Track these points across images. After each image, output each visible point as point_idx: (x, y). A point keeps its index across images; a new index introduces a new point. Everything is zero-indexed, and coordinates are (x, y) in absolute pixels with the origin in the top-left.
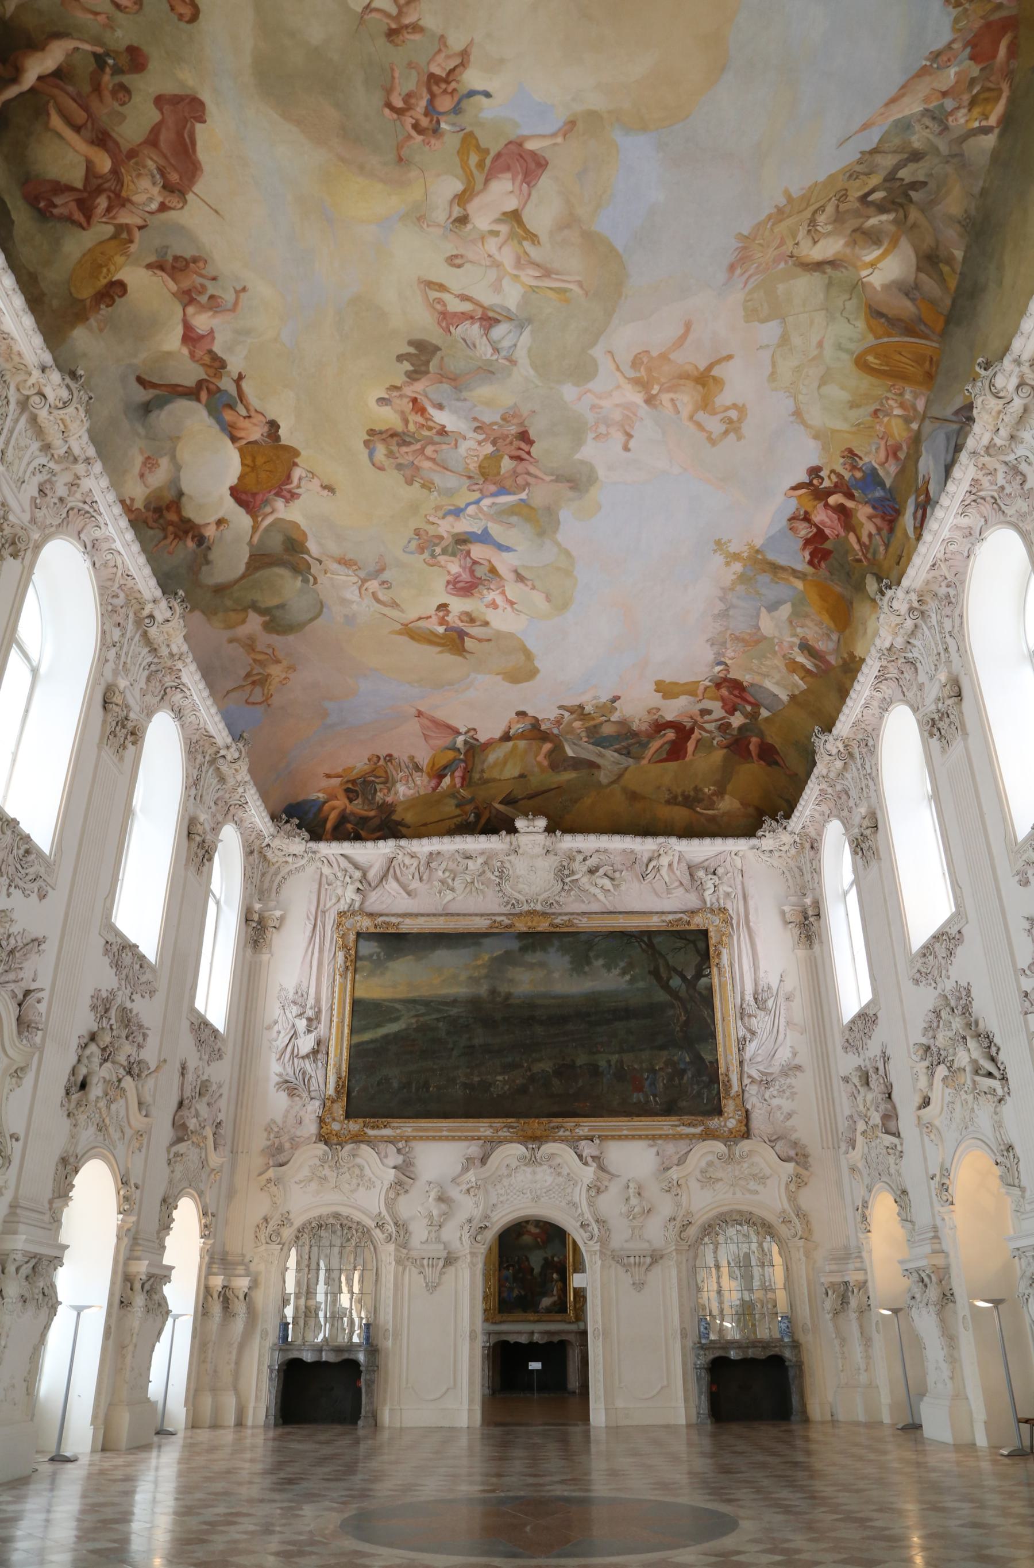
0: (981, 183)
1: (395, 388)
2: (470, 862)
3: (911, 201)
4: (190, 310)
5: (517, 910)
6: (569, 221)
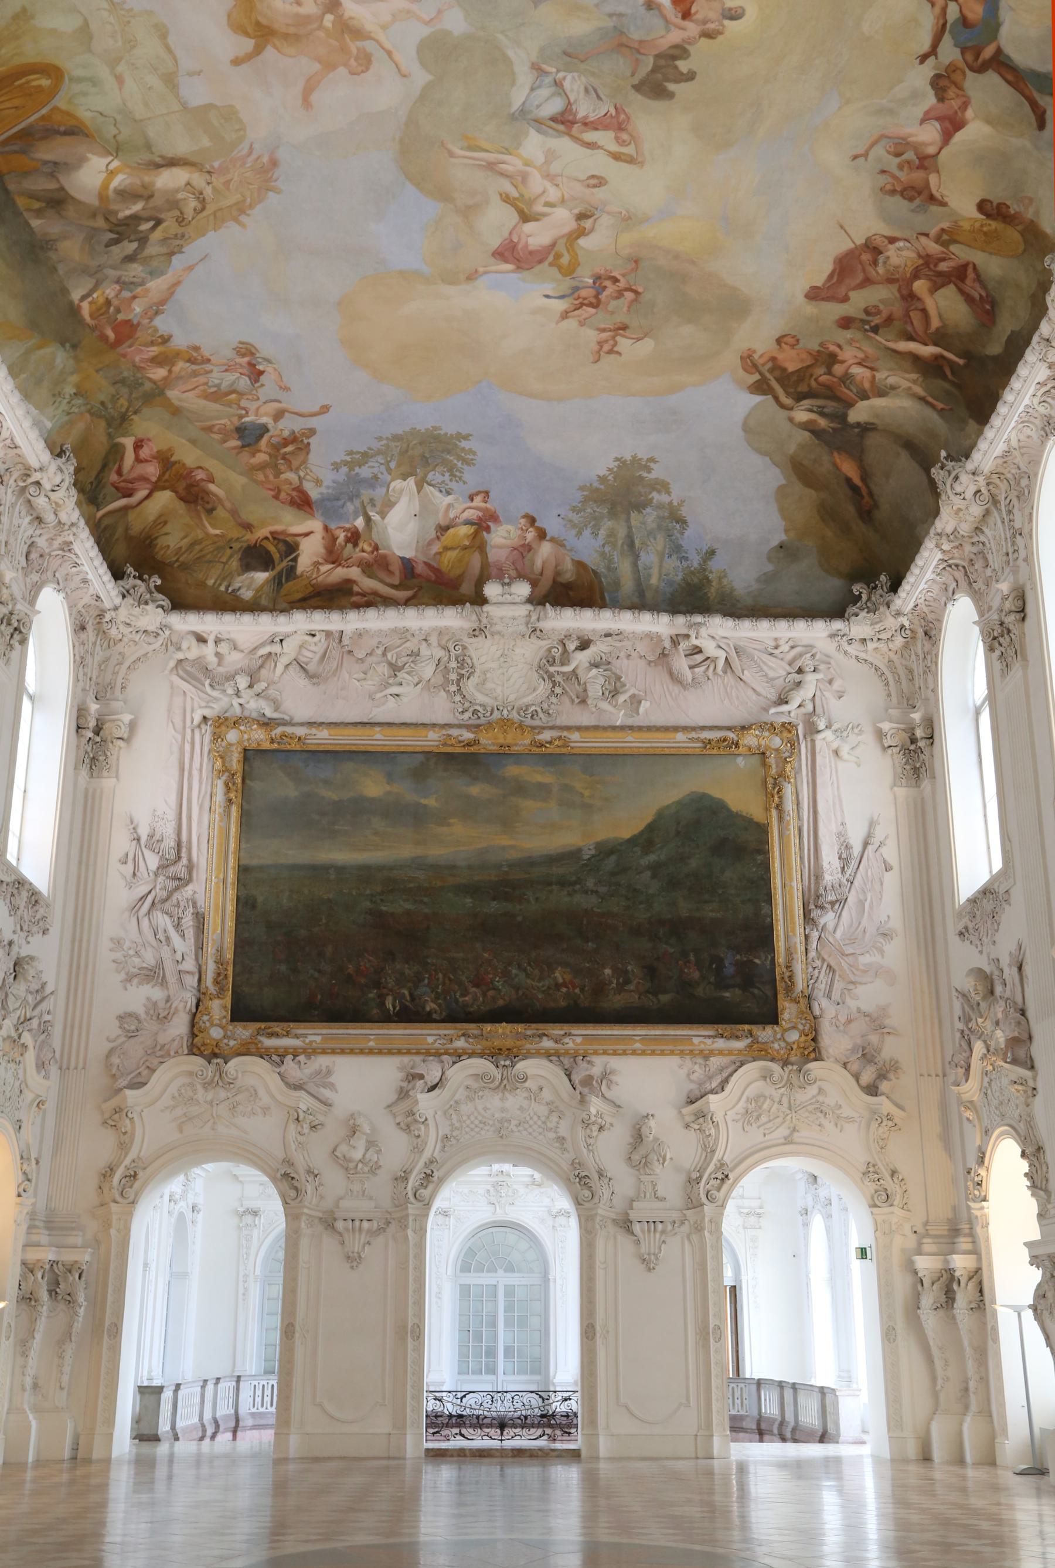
0: (61, 272)
1: (709, 35)
3: (111, 231)
4: (931, 150)
6: (469, 211)
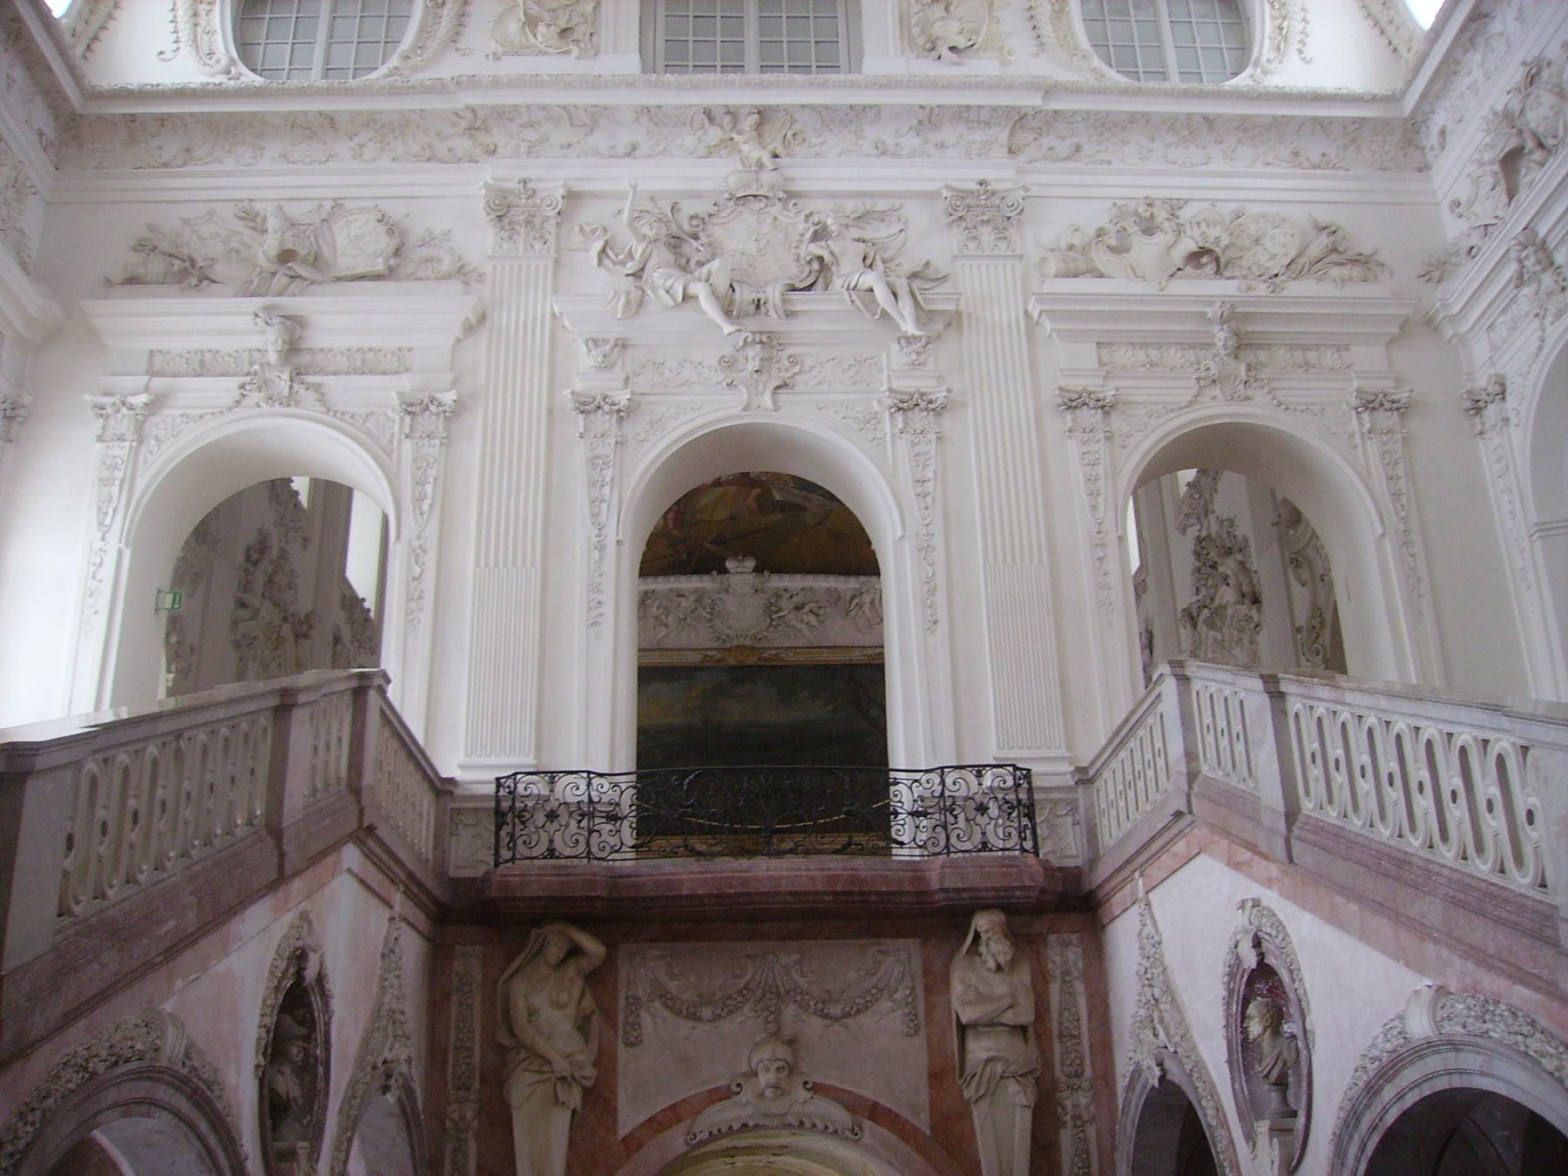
2: (683, 602)
5: (728, 645)
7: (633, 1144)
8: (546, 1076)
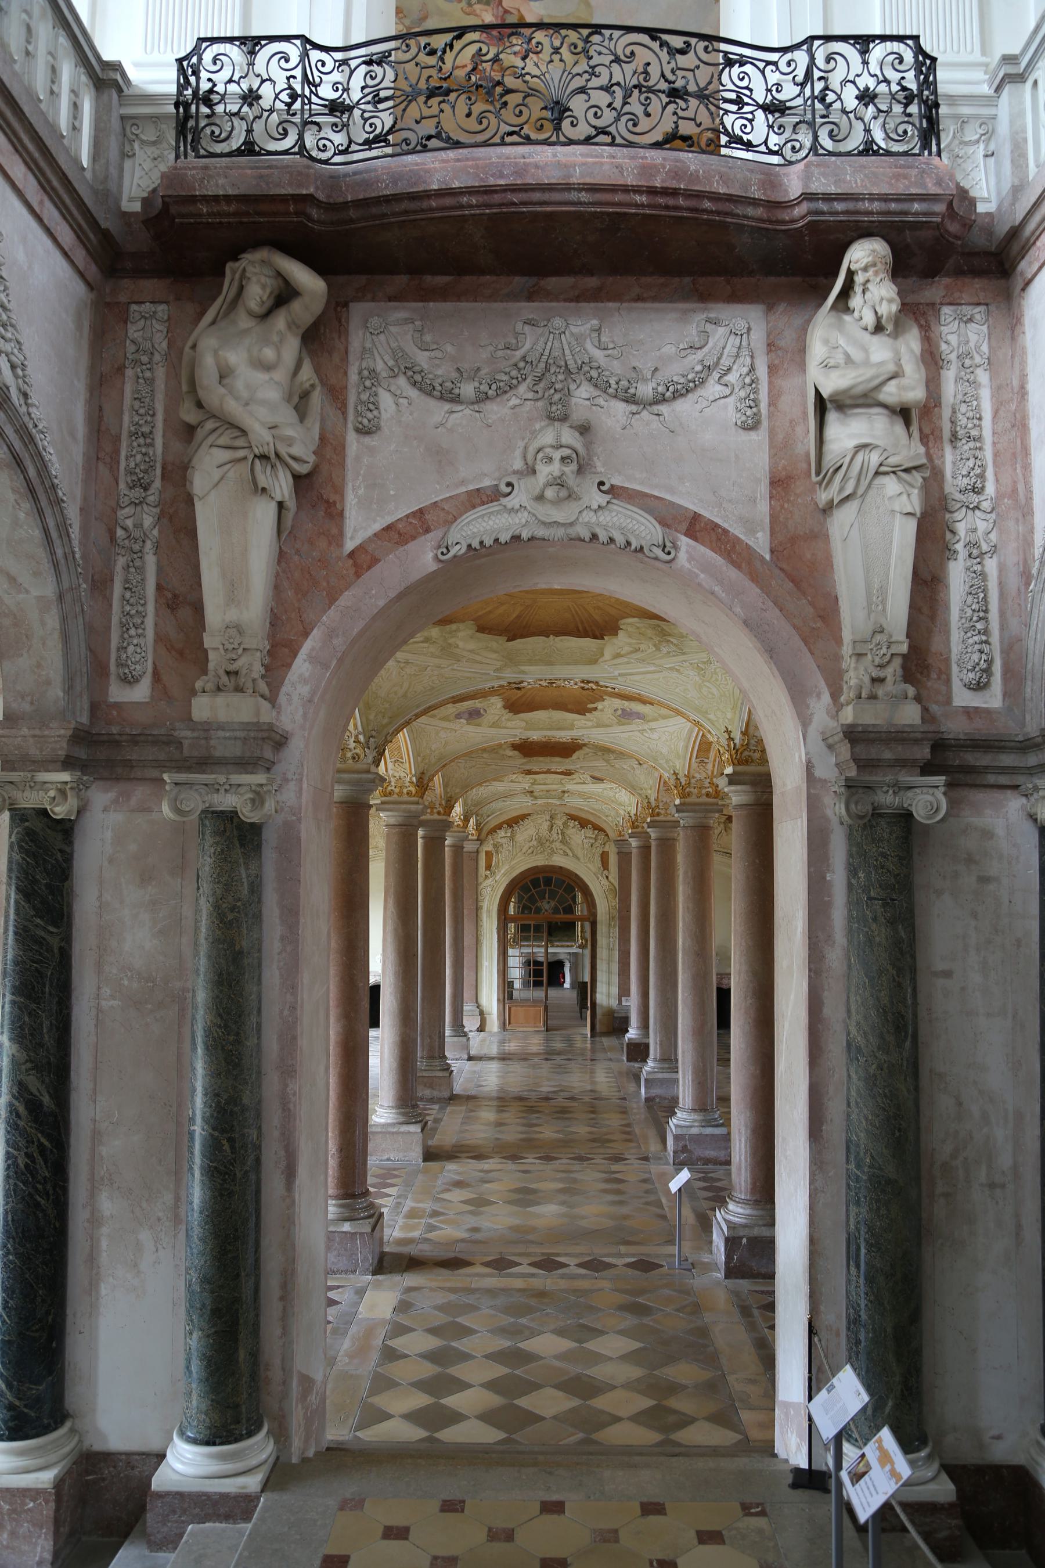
7: (363, 560)
8: (241, 454)
